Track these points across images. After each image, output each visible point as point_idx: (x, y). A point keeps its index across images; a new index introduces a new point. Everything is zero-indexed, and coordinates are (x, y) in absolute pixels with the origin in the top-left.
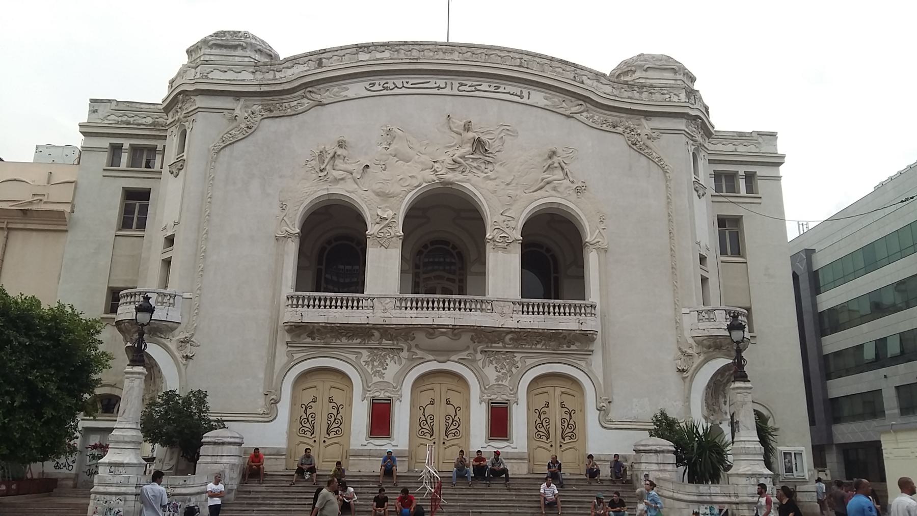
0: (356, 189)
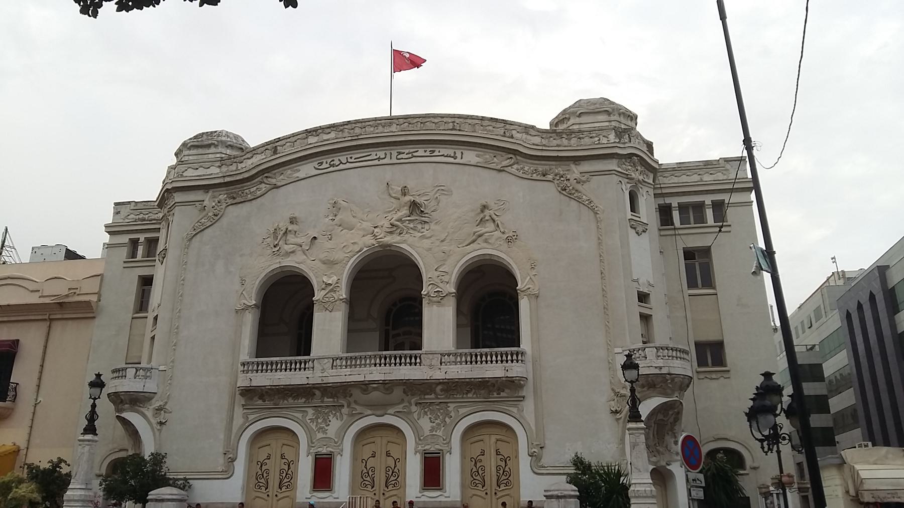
0: (305, 259)
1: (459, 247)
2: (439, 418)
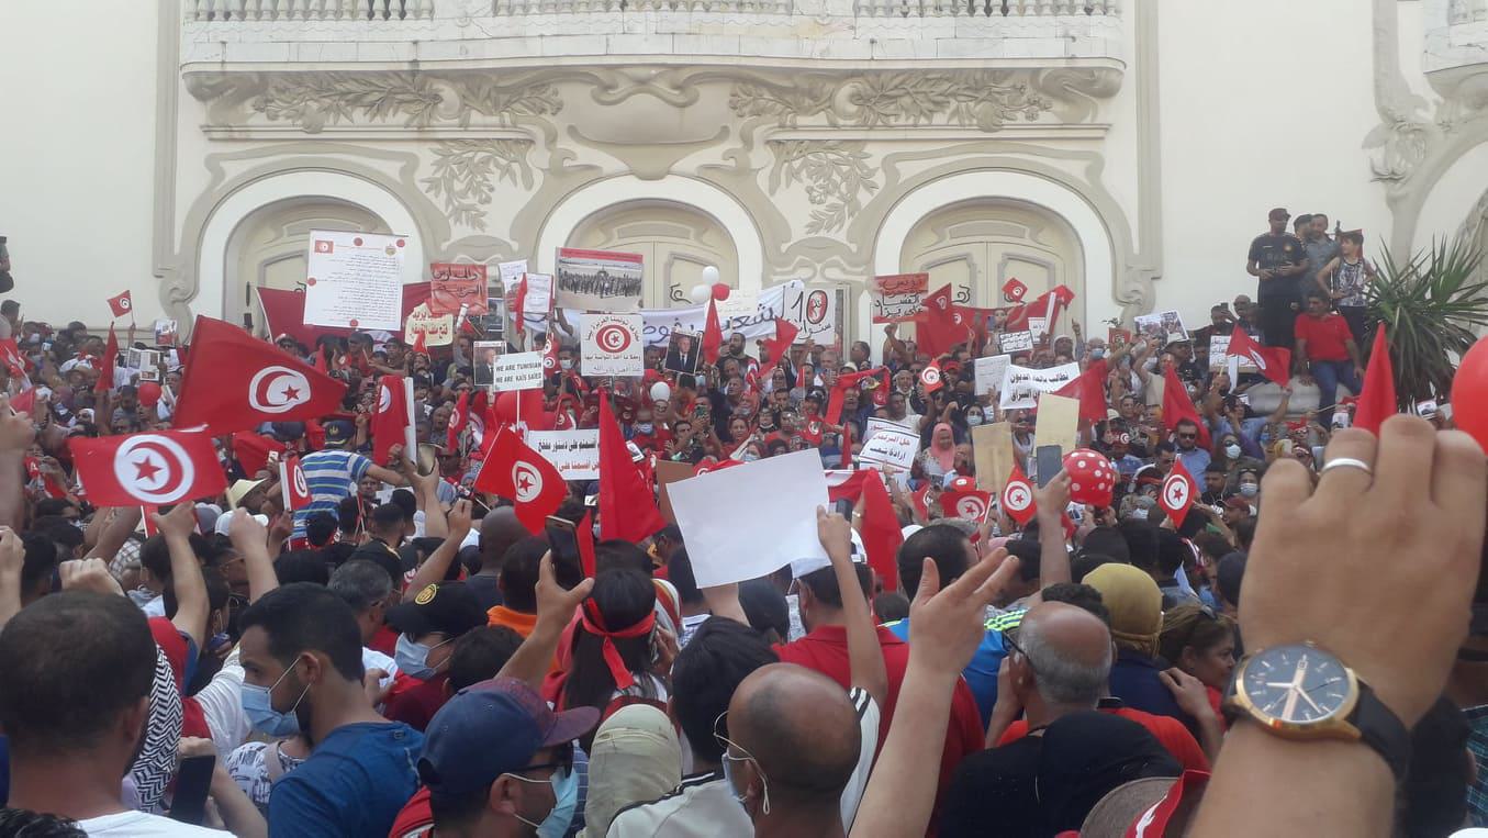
2: (837, 187)
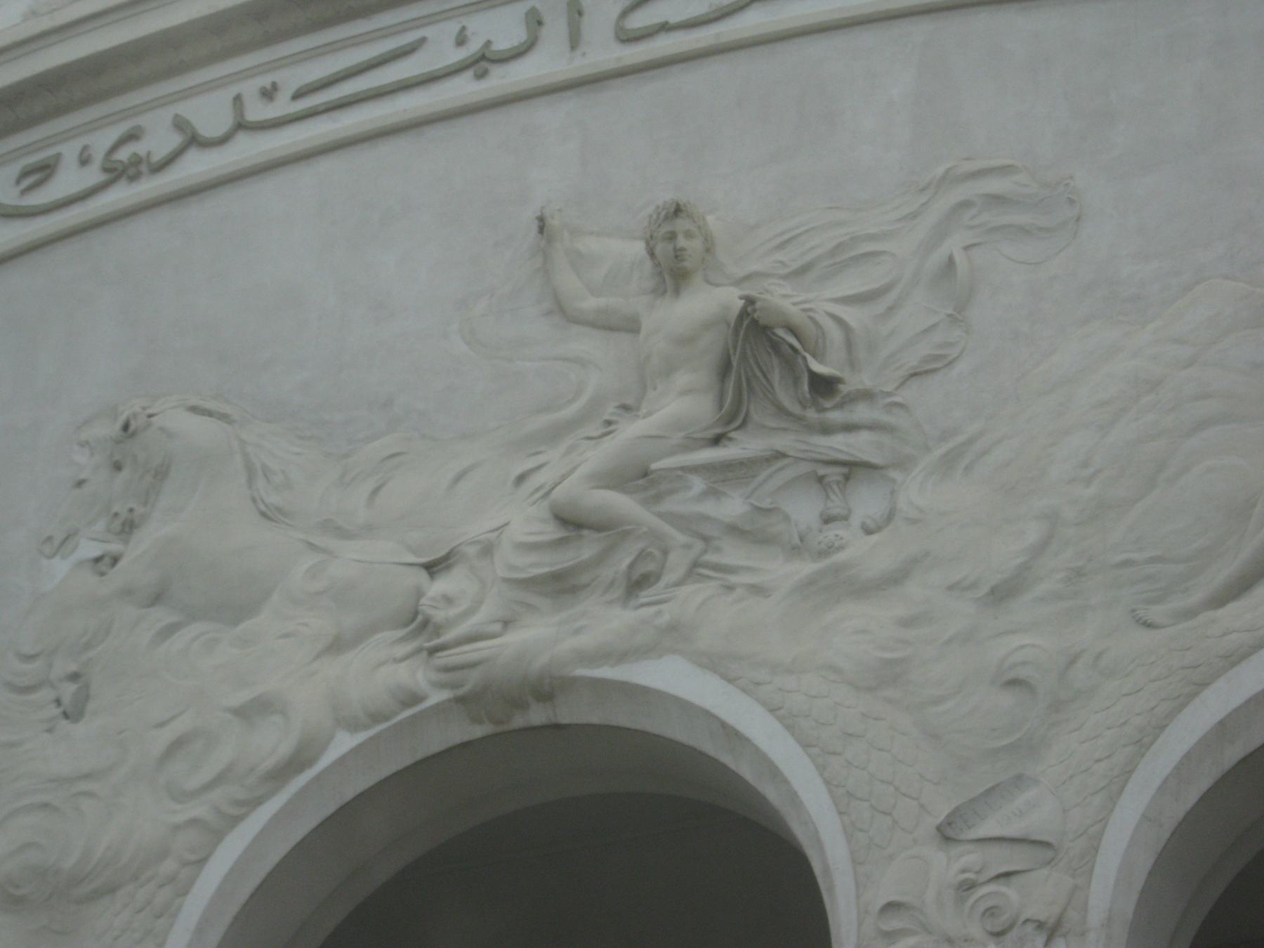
1: (1149, 625)
